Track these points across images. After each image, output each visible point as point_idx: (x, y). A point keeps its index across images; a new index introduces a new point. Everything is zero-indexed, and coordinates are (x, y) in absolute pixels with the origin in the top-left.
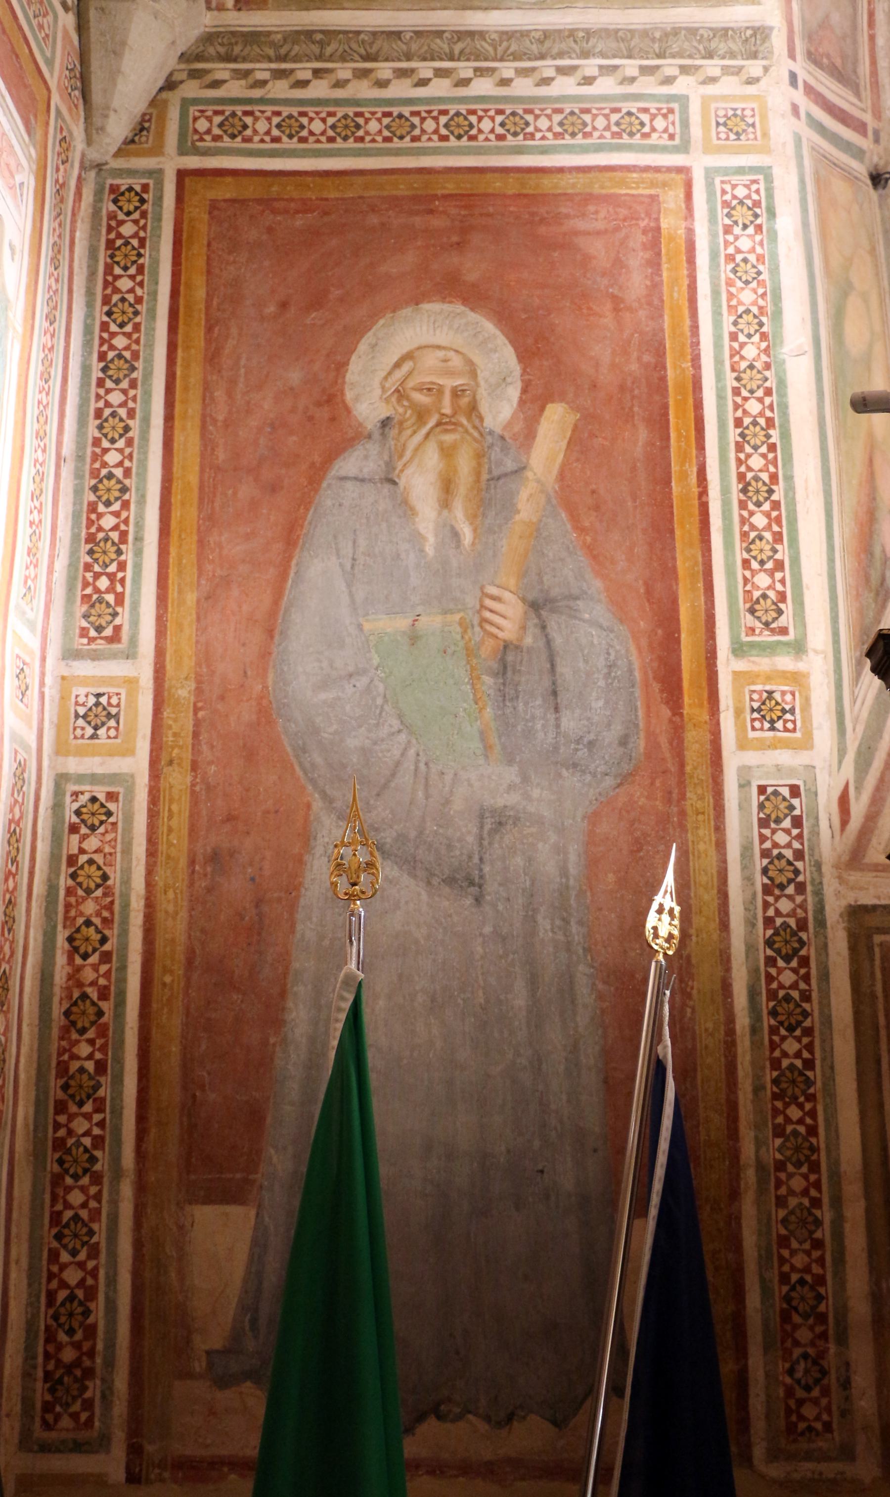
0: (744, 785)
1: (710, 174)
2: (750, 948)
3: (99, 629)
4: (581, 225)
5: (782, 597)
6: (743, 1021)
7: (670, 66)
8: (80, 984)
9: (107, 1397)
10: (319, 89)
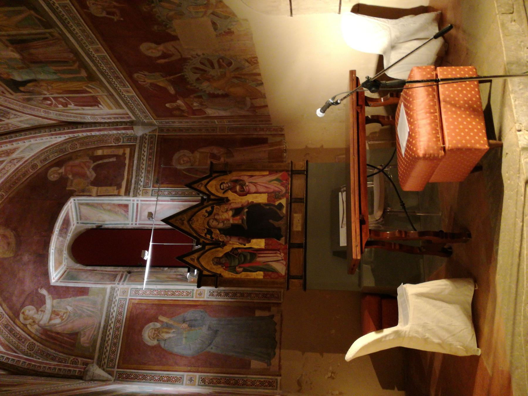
0: (208, 298)
1: (130, 296)
2: (227, 298)
3: (180, 380)
4: (135, 313)
5: (187, 292)
6: (235, 300)
7: (114, 300)
8: (224, 382)
9: (271, 379)
10: (108, 348)
